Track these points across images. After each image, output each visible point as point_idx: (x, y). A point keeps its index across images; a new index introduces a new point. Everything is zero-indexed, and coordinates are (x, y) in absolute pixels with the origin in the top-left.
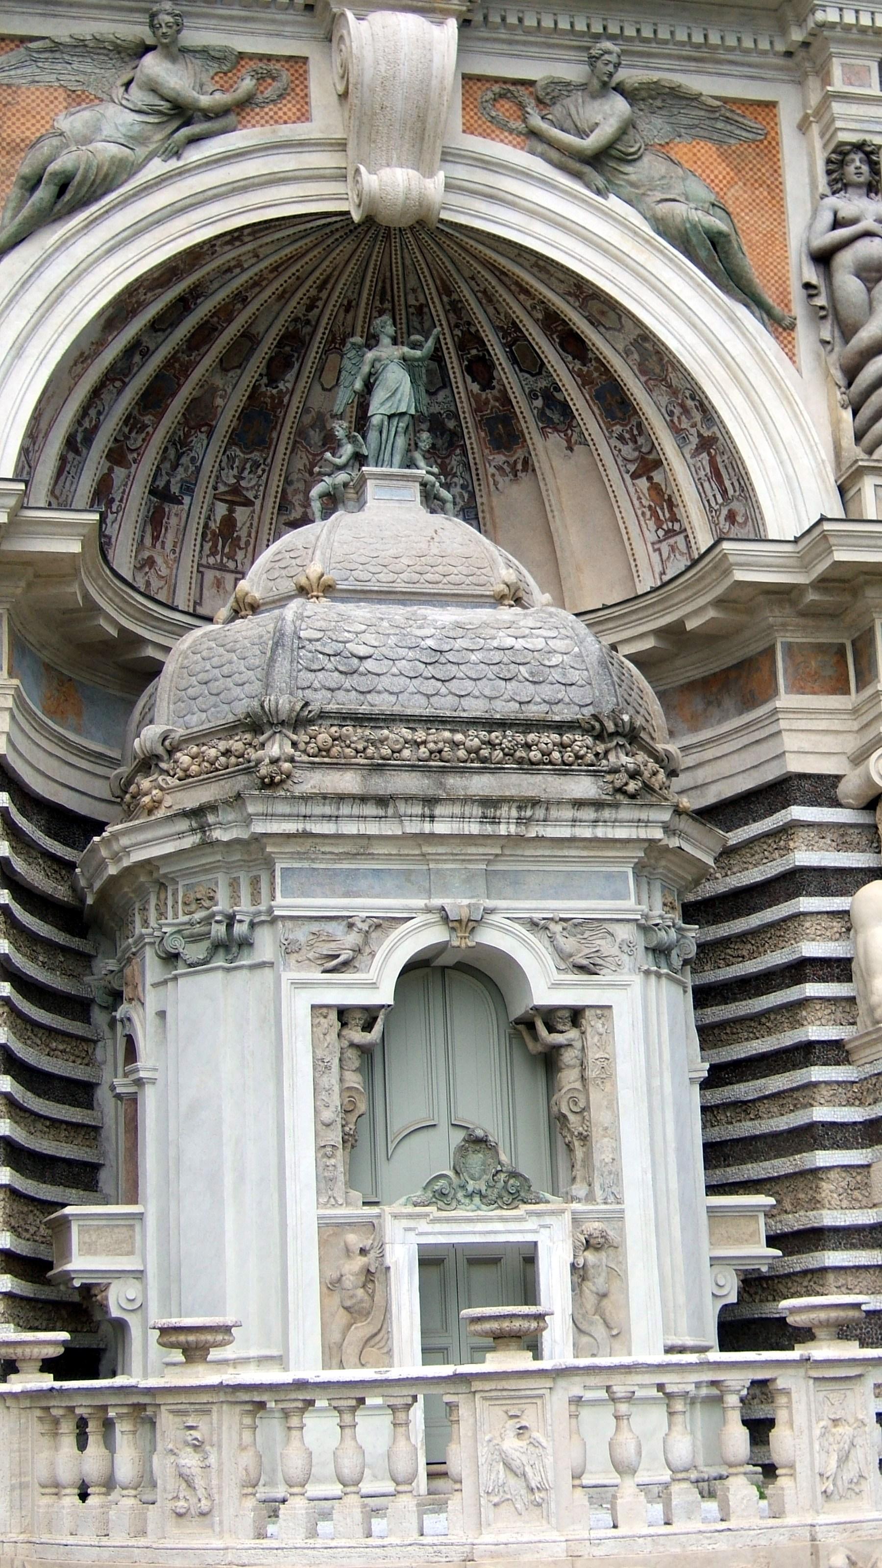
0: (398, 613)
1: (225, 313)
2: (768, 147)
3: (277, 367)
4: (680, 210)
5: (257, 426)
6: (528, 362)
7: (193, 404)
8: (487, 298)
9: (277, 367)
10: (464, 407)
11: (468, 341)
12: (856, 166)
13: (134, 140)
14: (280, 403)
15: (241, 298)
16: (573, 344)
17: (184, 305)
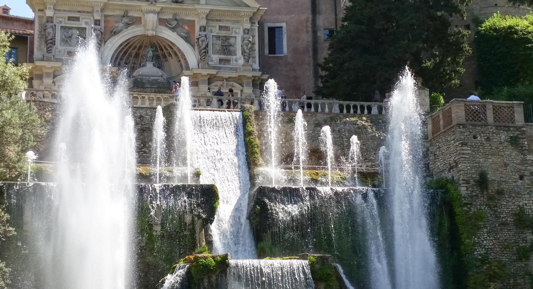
0: (148, 78)
1: (133, 44)
2: (194, 26)
3: (139, 49)
4: (183, 34)
5: (137, 55)
6: (166, 49)
7: (129, 54)
8: (162, 43)
9: (139, 49)
10: (160, 54)
11: (160, 47)
12: (202, 29)
13: (122, 27)
14: (139, 53)
15: (134, 43)
16: (171, 48)
17: (128, 44)
